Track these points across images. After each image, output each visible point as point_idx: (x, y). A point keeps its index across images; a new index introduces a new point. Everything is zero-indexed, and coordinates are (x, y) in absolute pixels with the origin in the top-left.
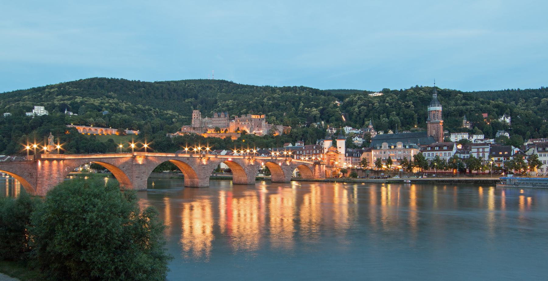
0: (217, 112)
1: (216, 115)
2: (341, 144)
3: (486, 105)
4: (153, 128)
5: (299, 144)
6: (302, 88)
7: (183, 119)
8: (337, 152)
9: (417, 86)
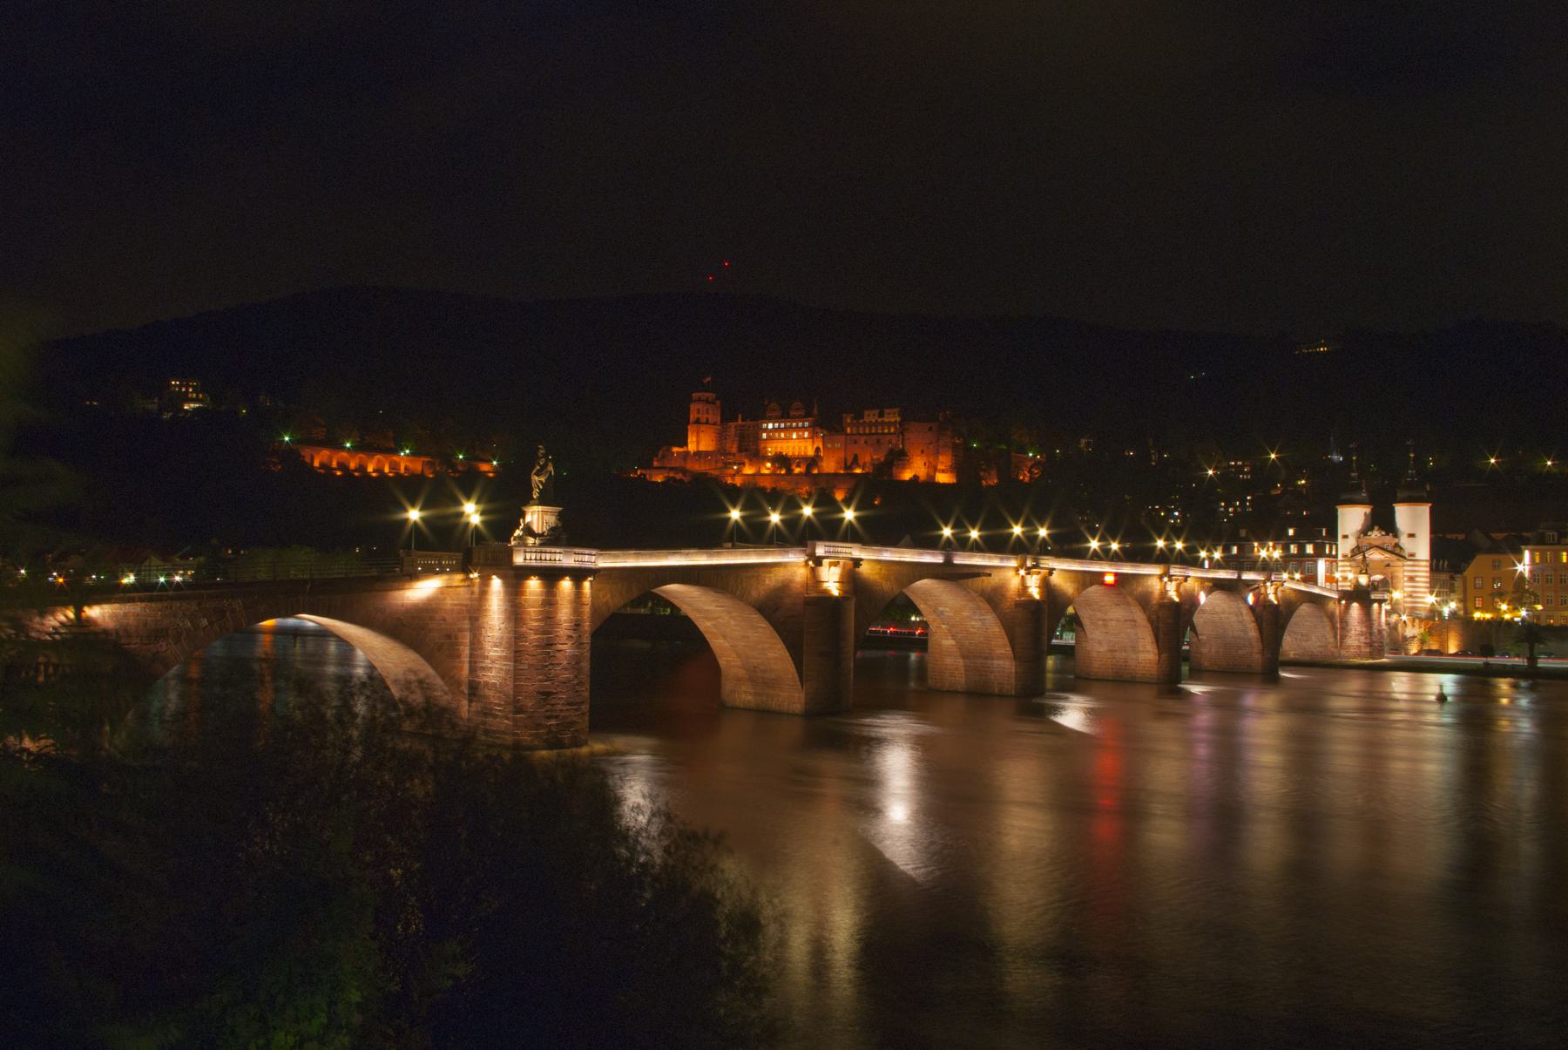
2: (1414, 521)
8: (1397, 551)
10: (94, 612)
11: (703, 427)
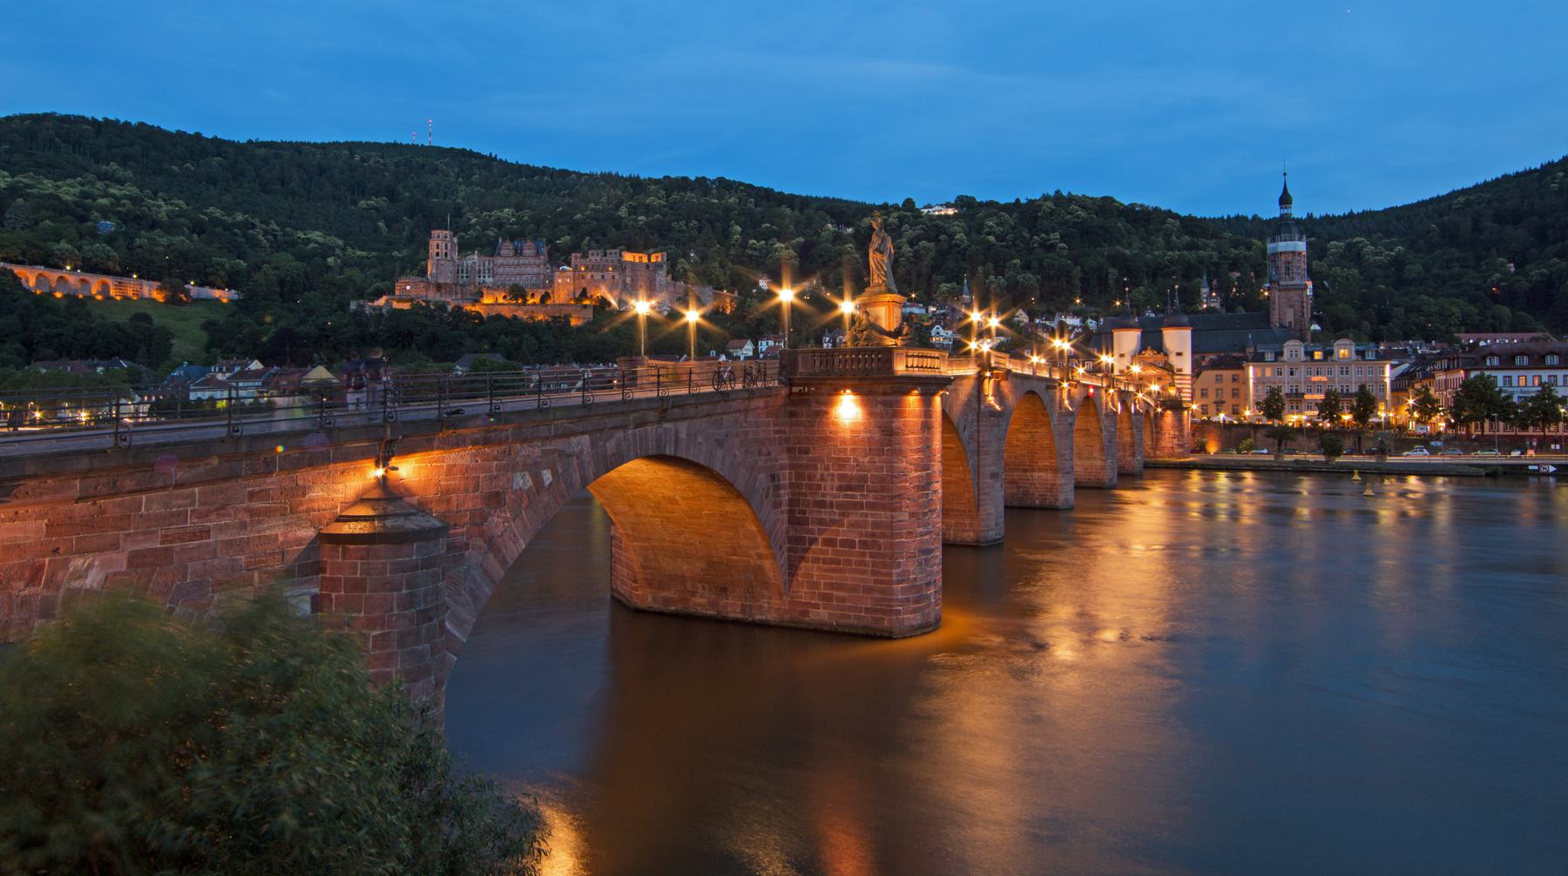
0: (512, 239)
1: (507, 248)
3: (1242, 251)
4: (281, 283)
5: (771, 343)
6: (725, 185)
7: (362, 258)
8: (1168, 368)
9: (1058, 192)
10: (408, 469)
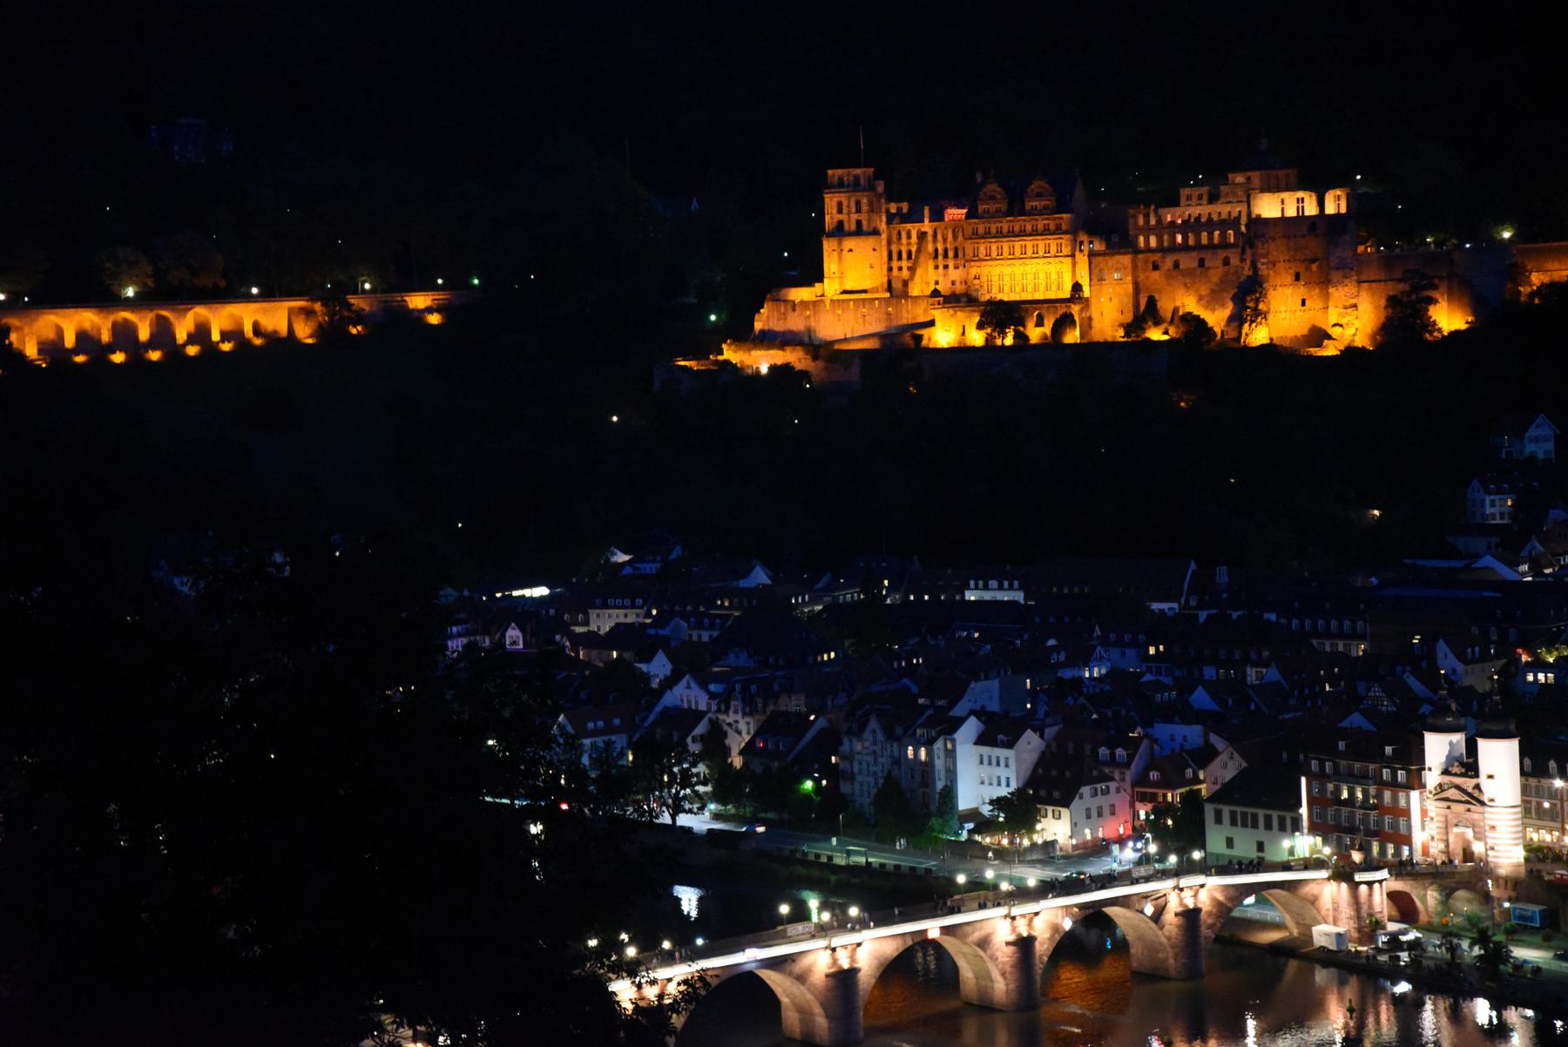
2: (1500, 759)
11: (849, 243)
